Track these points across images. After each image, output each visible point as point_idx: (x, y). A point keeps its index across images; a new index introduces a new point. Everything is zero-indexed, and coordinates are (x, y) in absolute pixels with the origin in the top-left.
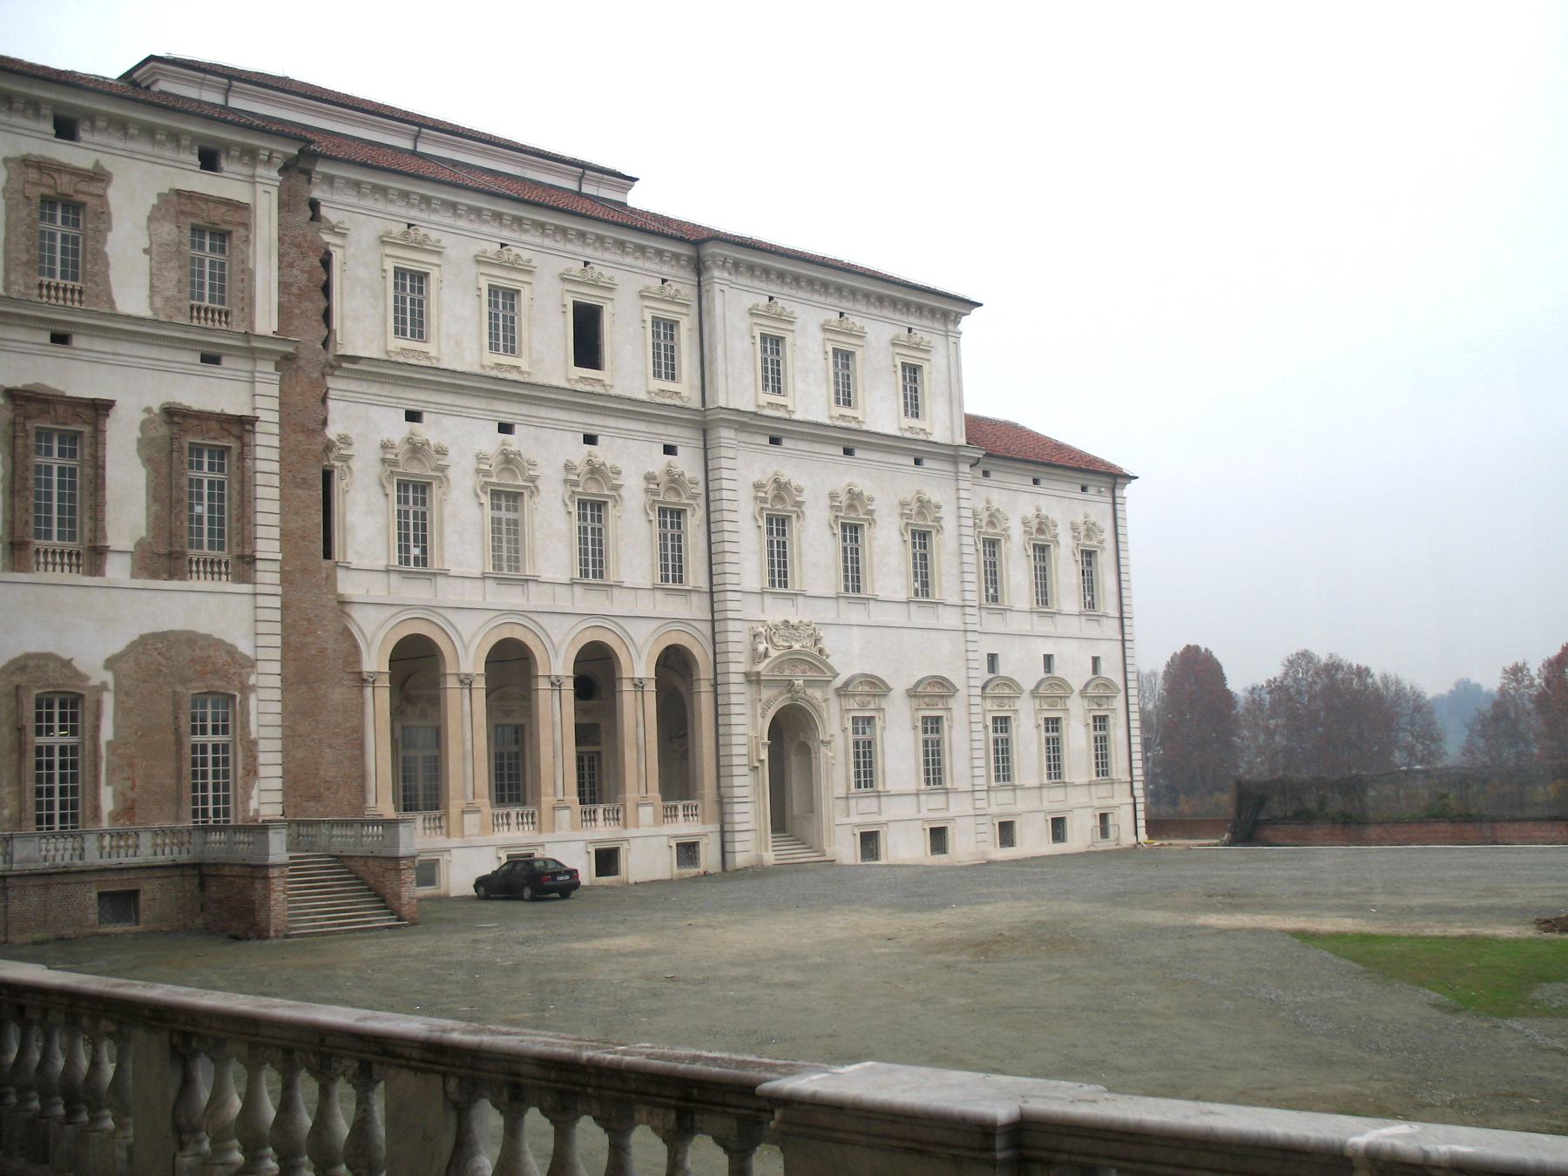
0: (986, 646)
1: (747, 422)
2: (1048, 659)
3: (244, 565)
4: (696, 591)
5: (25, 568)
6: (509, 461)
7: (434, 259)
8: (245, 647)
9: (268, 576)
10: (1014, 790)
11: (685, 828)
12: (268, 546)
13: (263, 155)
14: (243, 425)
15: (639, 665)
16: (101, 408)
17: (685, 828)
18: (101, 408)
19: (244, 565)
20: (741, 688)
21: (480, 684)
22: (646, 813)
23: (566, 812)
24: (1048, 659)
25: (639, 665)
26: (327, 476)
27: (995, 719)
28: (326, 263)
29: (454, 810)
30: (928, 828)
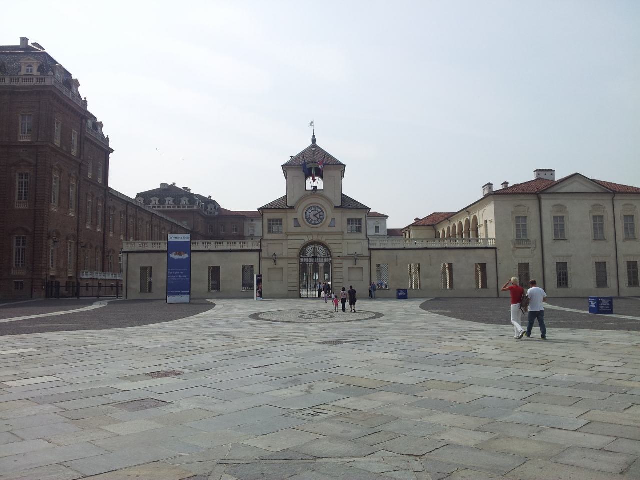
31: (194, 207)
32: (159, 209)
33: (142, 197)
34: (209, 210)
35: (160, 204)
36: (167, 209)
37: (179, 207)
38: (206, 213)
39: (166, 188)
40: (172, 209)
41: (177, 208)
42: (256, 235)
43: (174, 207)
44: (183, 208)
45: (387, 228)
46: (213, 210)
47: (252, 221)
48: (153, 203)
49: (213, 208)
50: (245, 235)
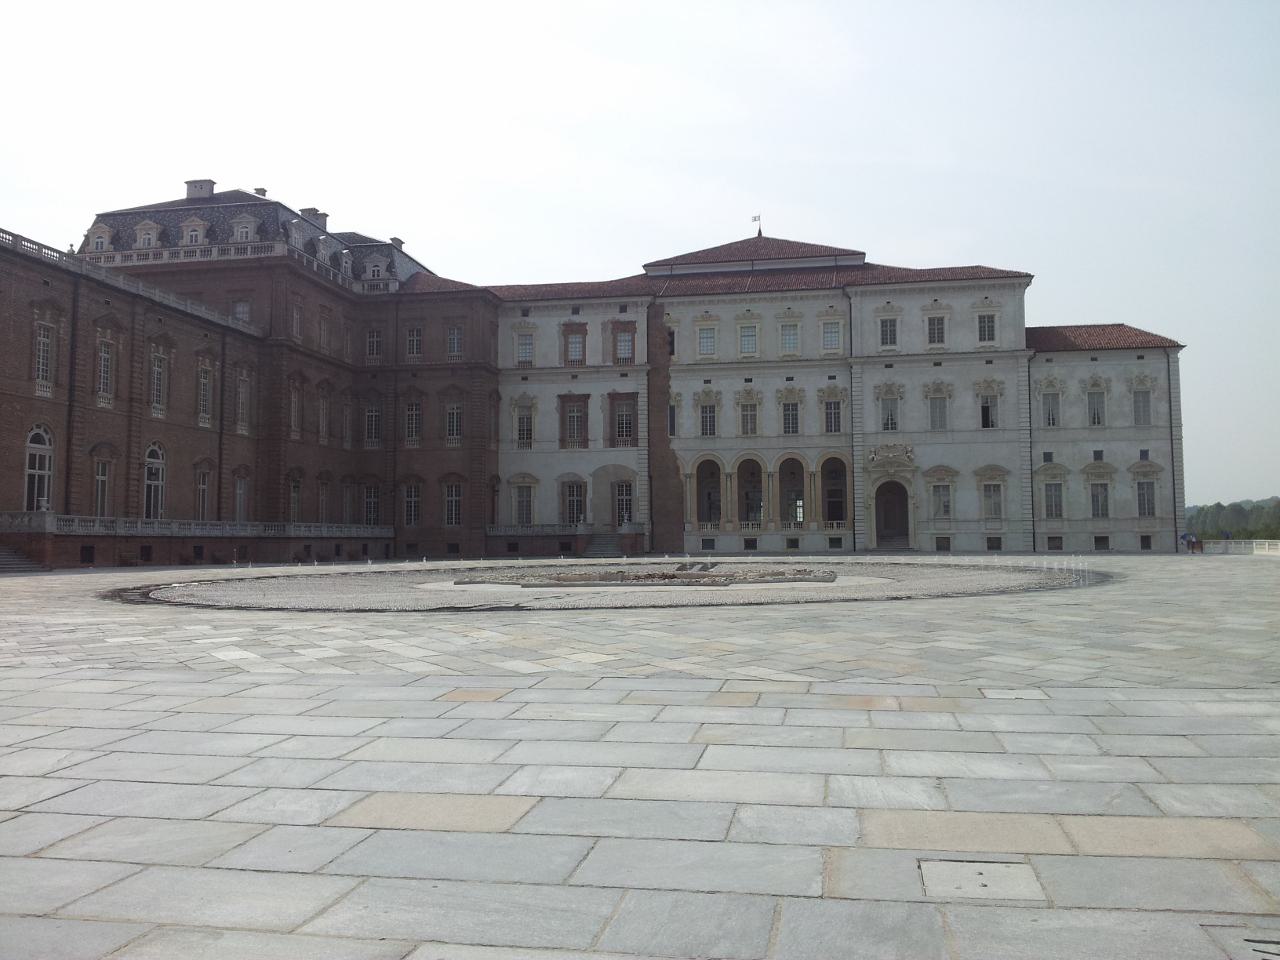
0: (1039, 451)
1: (868, 360)
2: (1098, 455)
3: (635, 443)
4: (846, 435)
5: (565, 448)
6: (749, 393)
7: (715, 322)
8: (635, 468)
9: (643, 443)
10: (1001, 521)
11: (835, 532)
12: (643, 433)
13: (639, 304)
14: (634, 396)
15: (813, 465)
16: (588, 396)
17: (835, 532)
18: (588, 396)
19: (635, 443)
20: (861, 475)
21: (735, 477)
22: (814, 525)
23: (773, 524)
24: (1098, 455)
25: (813, 465)
26: (672, 409)
27: (1047, 485)
28: (672, 334)
29: (723, 520)
30: (934, 537)
31: (271, 248)
32: (157, 262)
33: (111, 226)
34: (369, 275)
35: (163, 246)
36: (182, 259)
37: (223, 252)
38: (357, 288)
39: (204, 194)
40: (198, 258)
41: (215, 255)
42: (538, 363)
43: (206, 252)
44: (253, 252)
45: (1031, 322)
46: (383, 274)
47: (525, 313)
48: (140, 243)
49: (383, 268)
50: (500, 366)
